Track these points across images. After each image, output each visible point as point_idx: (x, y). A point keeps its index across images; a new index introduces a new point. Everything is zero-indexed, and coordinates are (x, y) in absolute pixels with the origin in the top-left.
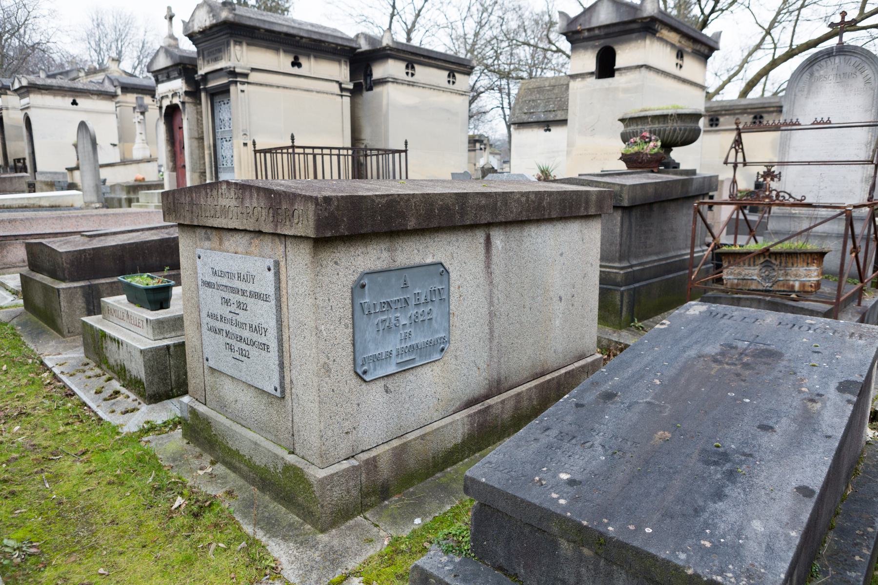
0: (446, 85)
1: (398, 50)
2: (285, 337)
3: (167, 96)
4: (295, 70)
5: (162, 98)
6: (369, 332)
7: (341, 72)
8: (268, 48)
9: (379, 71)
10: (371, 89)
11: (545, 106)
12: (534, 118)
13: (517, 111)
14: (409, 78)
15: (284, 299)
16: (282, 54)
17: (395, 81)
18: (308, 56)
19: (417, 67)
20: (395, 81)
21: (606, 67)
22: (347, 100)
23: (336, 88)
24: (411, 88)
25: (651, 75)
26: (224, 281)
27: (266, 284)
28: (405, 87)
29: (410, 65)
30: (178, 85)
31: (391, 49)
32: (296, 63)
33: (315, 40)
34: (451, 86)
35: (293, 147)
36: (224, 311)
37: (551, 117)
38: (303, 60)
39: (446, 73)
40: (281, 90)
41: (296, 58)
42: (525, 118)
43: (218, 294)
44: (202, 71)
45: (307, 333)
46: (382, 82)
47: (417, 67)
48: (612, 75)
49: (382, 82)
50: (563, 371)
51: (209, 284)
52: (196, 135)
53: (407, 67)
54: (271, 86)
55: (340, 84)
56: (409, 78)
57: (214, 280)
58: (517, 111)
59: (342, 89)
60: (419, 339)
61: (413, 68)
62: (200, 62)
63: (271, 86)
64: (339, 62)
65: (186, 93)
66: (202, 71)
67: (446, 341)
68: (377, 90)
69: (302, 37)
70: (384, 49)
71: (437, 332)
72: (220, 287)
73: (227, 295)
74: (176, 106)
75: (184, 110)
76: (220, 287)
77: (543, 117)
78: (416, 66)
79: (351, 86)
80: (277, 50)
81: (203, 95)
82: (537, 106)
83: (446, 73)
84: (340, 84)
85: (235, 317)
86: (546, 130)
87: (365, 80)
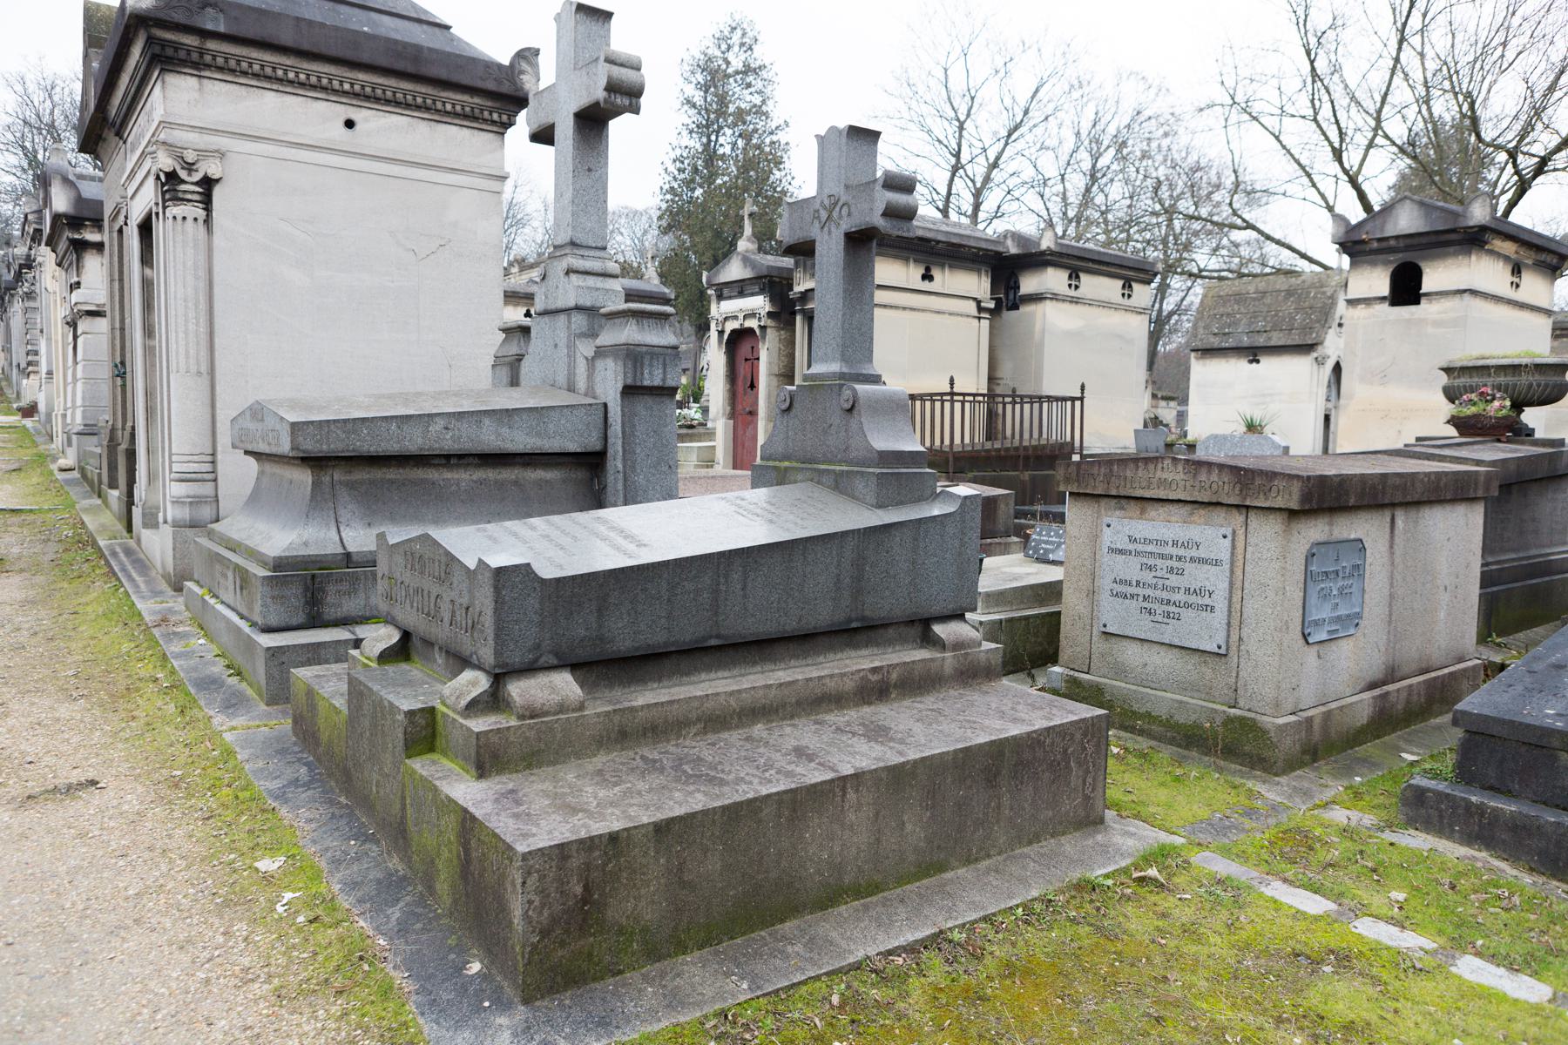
0: (1119, 300)
1: (1061, 254)
2: (1237, 598)
3: (736, 318)
4: (926, 286)
5: (726, 319)
6: (1313, 600)
7: (978, 285)
8: (896, 257)
9: (1029, 284)
10: (1015, 307)
11: (1250, 324)
12: (1230, 343)
13: (1201, 331)
14: (1072, 293)
15: (1240, 564)
16: (912, 265)
17: (1055, 297)
18: (942, 266)
19: (1084, 277)
20: (1055, 297)
21: (1406, 289)
22: (985, 324)
23: (971, 307)
24: (1073, 306)
25: (1478, 303)
26: (1150, 548)
27: (1222, 549)
28: (1066, 306)
29: (1074, 275)
30: (759, 303)
31: (1052, 253)
32: (927, 277)
33: (953, 245)
34: (1126, 302)
35: (952, 394)
36: (1148, 577)
37: (1261, 340)
38: (936, 272)
39: (1120, 283)
40: (907, 313)
41: (928, 269)
42: (1215, 342)
43: (1135, 562)
44: (799, 288)
45: (1271, 594)
46: (1036, 298)
47: (1084, 277)
48: (1417, 302)
49: (1036, 298)
50: (1446, 671)
51: (1121, 552)
52: (776, 371)
53: (1070, 277)
54: (896, 307)
55: (978, 302)
56: (1072, 293)
57: (1131, 547)
58: (1201, 331)
59: (980, 309)
60: (1342, 611)
61: (1078, 277)
62: (798, 275)
63: (896, 307)
64: (979, 272)
65: (770, 314)
66: (799, 288)
67: (1359, 616)
68: (1026, 309)
69: (938, 242)
70: (1043, 253)
71: (1353, 606)
72: (1138, 553)
73: (1151, 562)
74: (751, 331)
75: (764, 338)
76: (1138, 553)
77: (1246, 341)
78: (1082, 275)
79: (992, 305)
80: (907, 260)
81: (799, 318)
82: (1236, 323)
83: (1120, 283)
84: (978, 302)
85: (1160, 582)
86: (1251, 362)
87: (1007, 295)
